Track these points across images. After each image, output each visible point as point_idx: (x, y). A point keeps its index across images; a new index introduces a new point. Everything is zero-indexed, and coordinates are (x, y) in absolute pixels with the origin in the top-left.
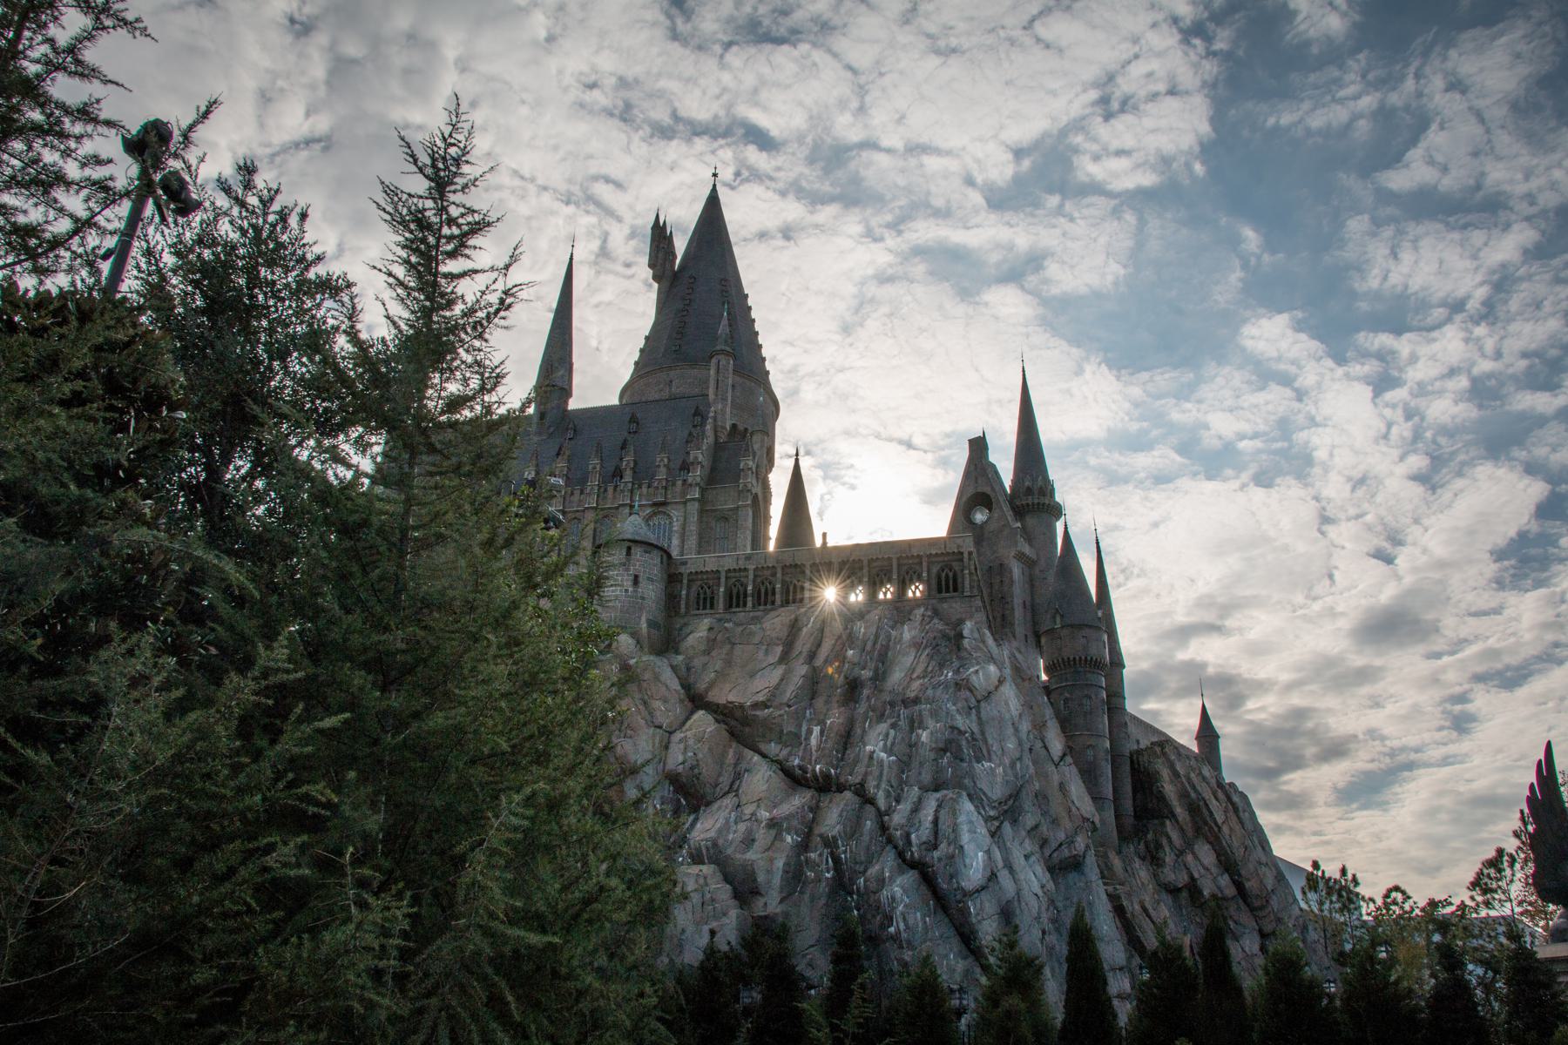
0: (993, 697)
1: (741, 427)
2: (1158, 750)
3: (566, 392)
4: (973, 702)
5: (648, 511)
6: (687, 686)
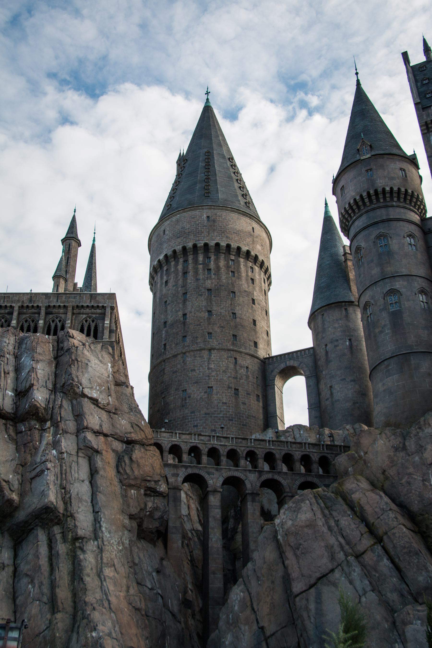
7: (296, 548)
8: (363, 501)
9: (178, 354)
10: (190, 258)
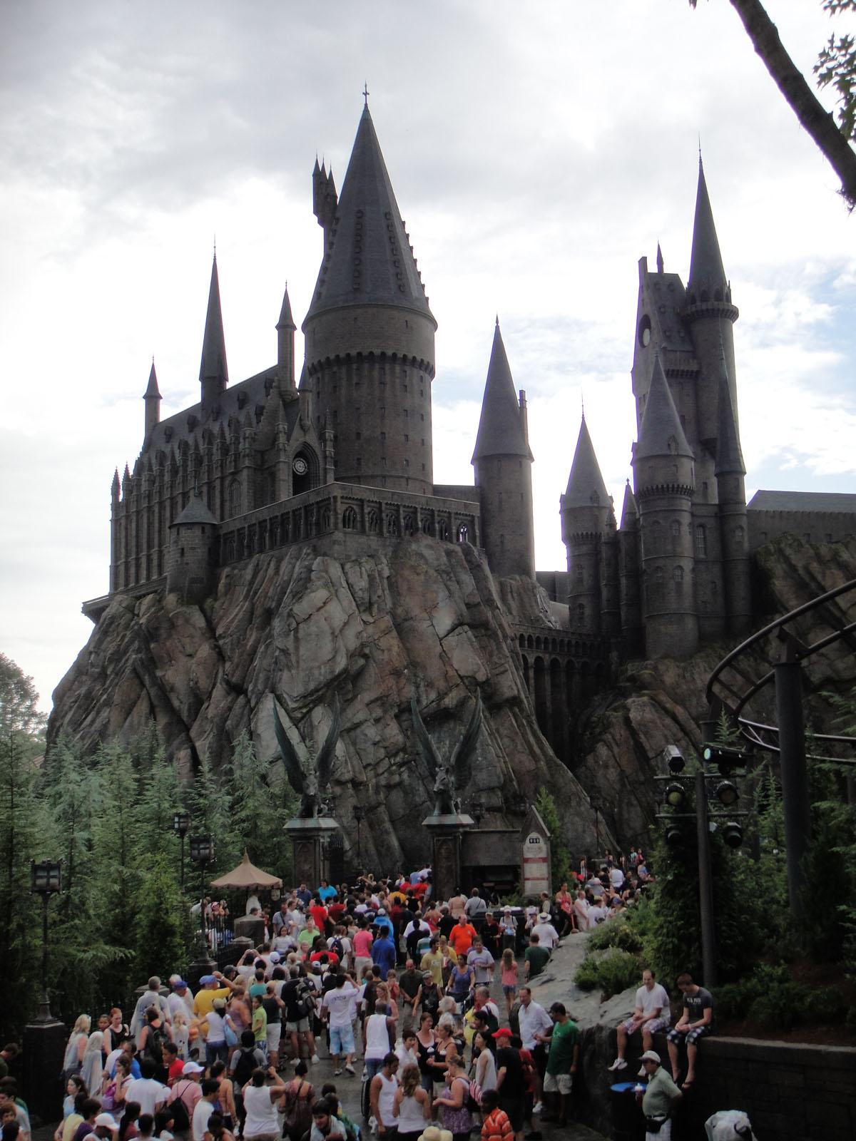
0: (312, 617)
1: (365, 353)
2: (772, 548)
3: (223, 377)
4: (294, 625)
5: (229, 478)
6: (209, 621)
7: (646, 734)
8: (676, 711)
9: (377, 476)
10: (387, 367)
